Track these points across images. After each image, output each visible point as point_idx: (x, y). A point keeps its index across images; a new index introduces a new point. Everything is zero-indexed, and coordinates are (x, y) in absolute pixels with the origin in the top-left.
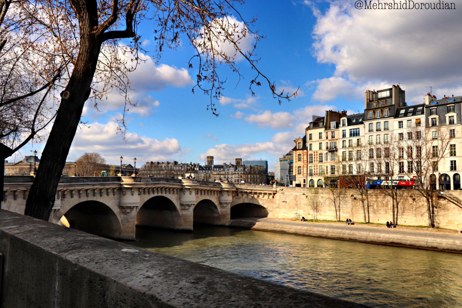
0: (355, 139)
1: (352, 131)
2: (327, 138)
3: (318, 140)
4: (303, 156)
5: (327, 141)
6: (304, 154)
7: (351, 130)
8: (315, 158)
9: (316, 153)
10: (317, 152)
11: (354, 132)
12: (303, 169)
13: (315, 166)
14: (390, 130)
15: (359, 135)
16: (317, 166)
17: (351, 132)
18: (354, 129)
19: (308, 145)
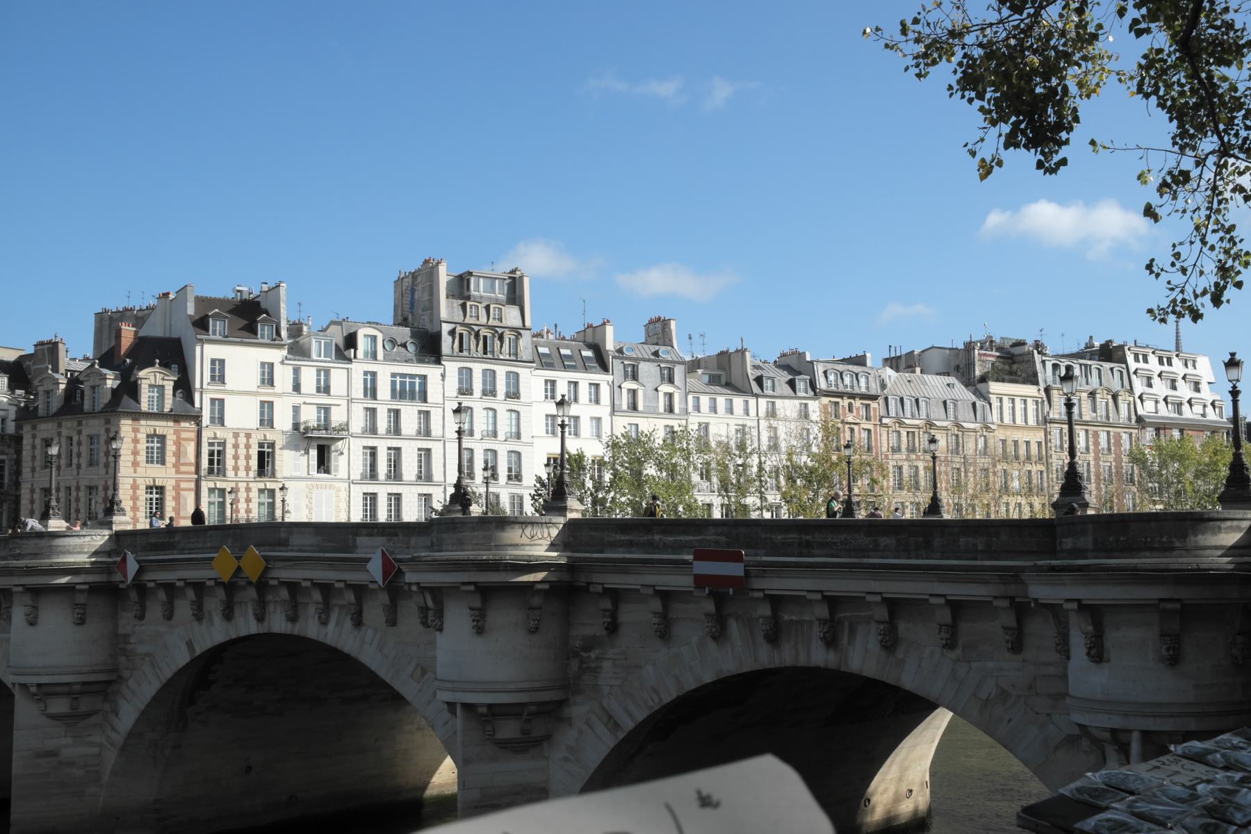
0: (410, 414)
1: (398, 379)
2: (297, 388)
3: (255, 389)
5: (298, 400)
6: (184, 435)
7: (393, 375)
8: (236, 457)
9: (242, 440)
10: (248, 436)
11: (403, 384)
14: (522, 399)
15: (424, 399)
16: (248, 490)
17: (393, 383)
18: (403, 376)
19: (203, 402)
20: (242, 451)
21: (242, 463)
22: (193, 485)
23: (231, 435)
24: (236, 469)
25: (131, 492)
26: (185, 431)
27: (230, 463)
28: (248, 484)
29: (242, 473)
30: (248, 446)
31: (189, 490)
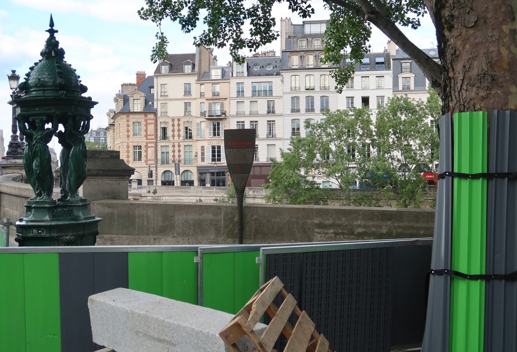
3: (183, 97)
4: (146, 125)
6: (149, 122)
9: (176, 122)
10: (179, 120)
12: (146, 151)
13: (174, 146)
15: (271, 94)
20: (176, 128)
21: (176, 133)
22: (153, 145)
23: (171, 120)
24: (173, 136)
25: (126, 149)
26: (149, 120)
27: (169, 133)
28: (179, 143)
29: (176, 138)
30: (179, 125)
31: (152, 147)
